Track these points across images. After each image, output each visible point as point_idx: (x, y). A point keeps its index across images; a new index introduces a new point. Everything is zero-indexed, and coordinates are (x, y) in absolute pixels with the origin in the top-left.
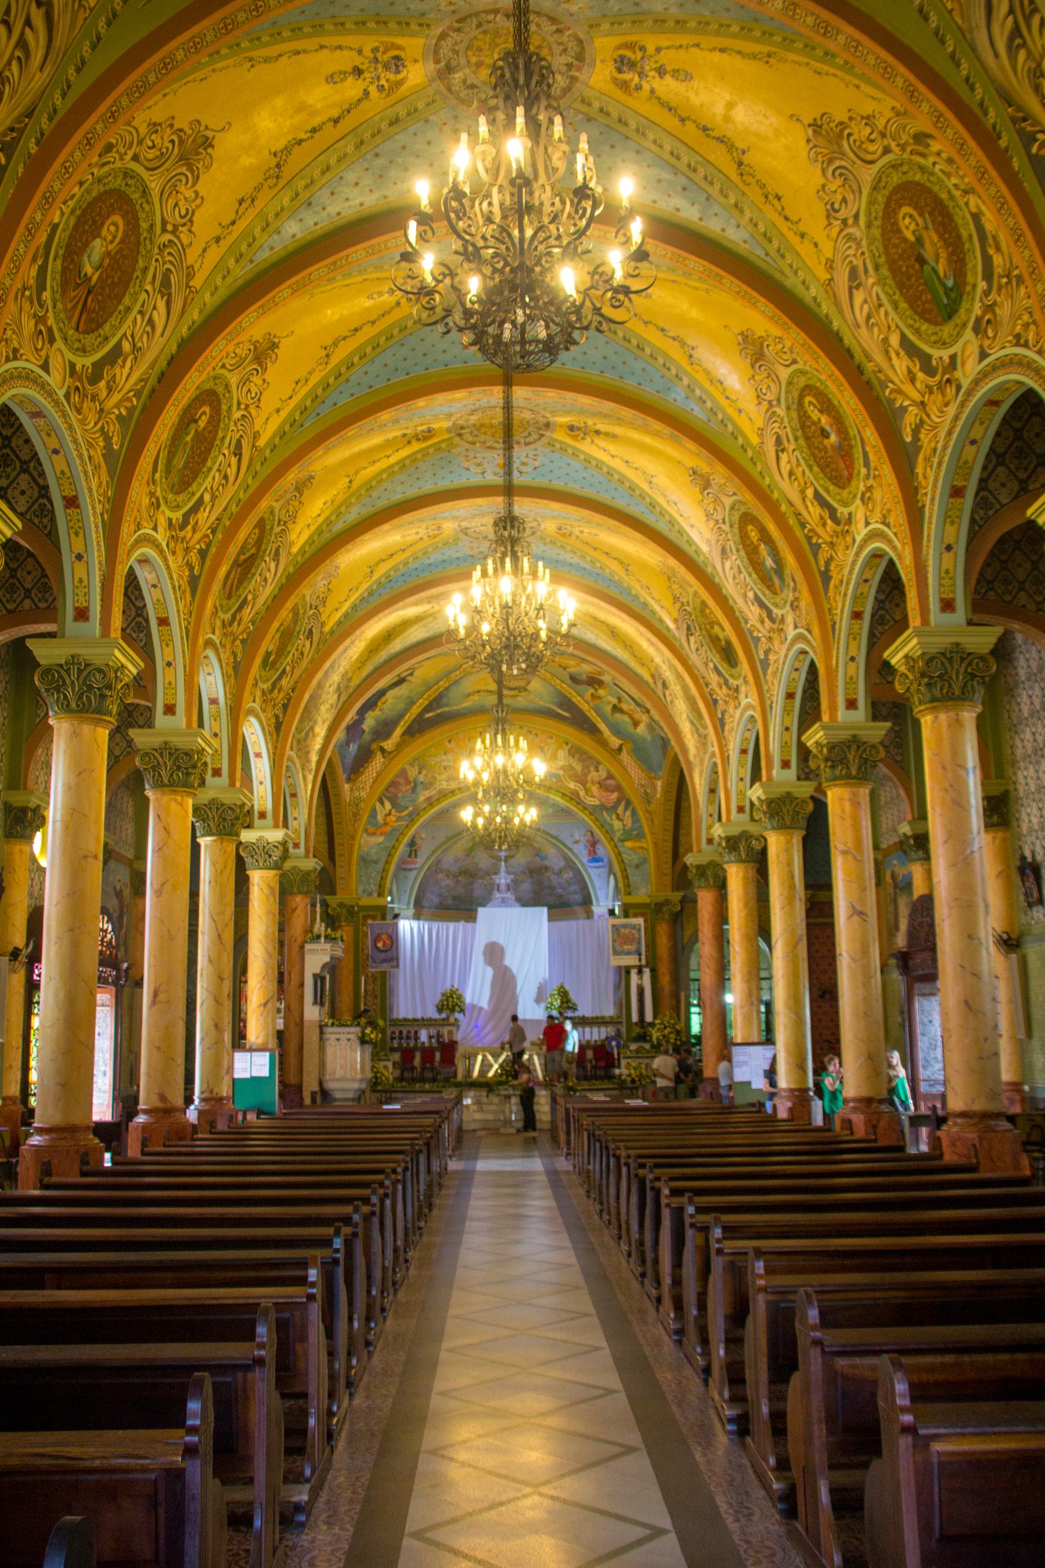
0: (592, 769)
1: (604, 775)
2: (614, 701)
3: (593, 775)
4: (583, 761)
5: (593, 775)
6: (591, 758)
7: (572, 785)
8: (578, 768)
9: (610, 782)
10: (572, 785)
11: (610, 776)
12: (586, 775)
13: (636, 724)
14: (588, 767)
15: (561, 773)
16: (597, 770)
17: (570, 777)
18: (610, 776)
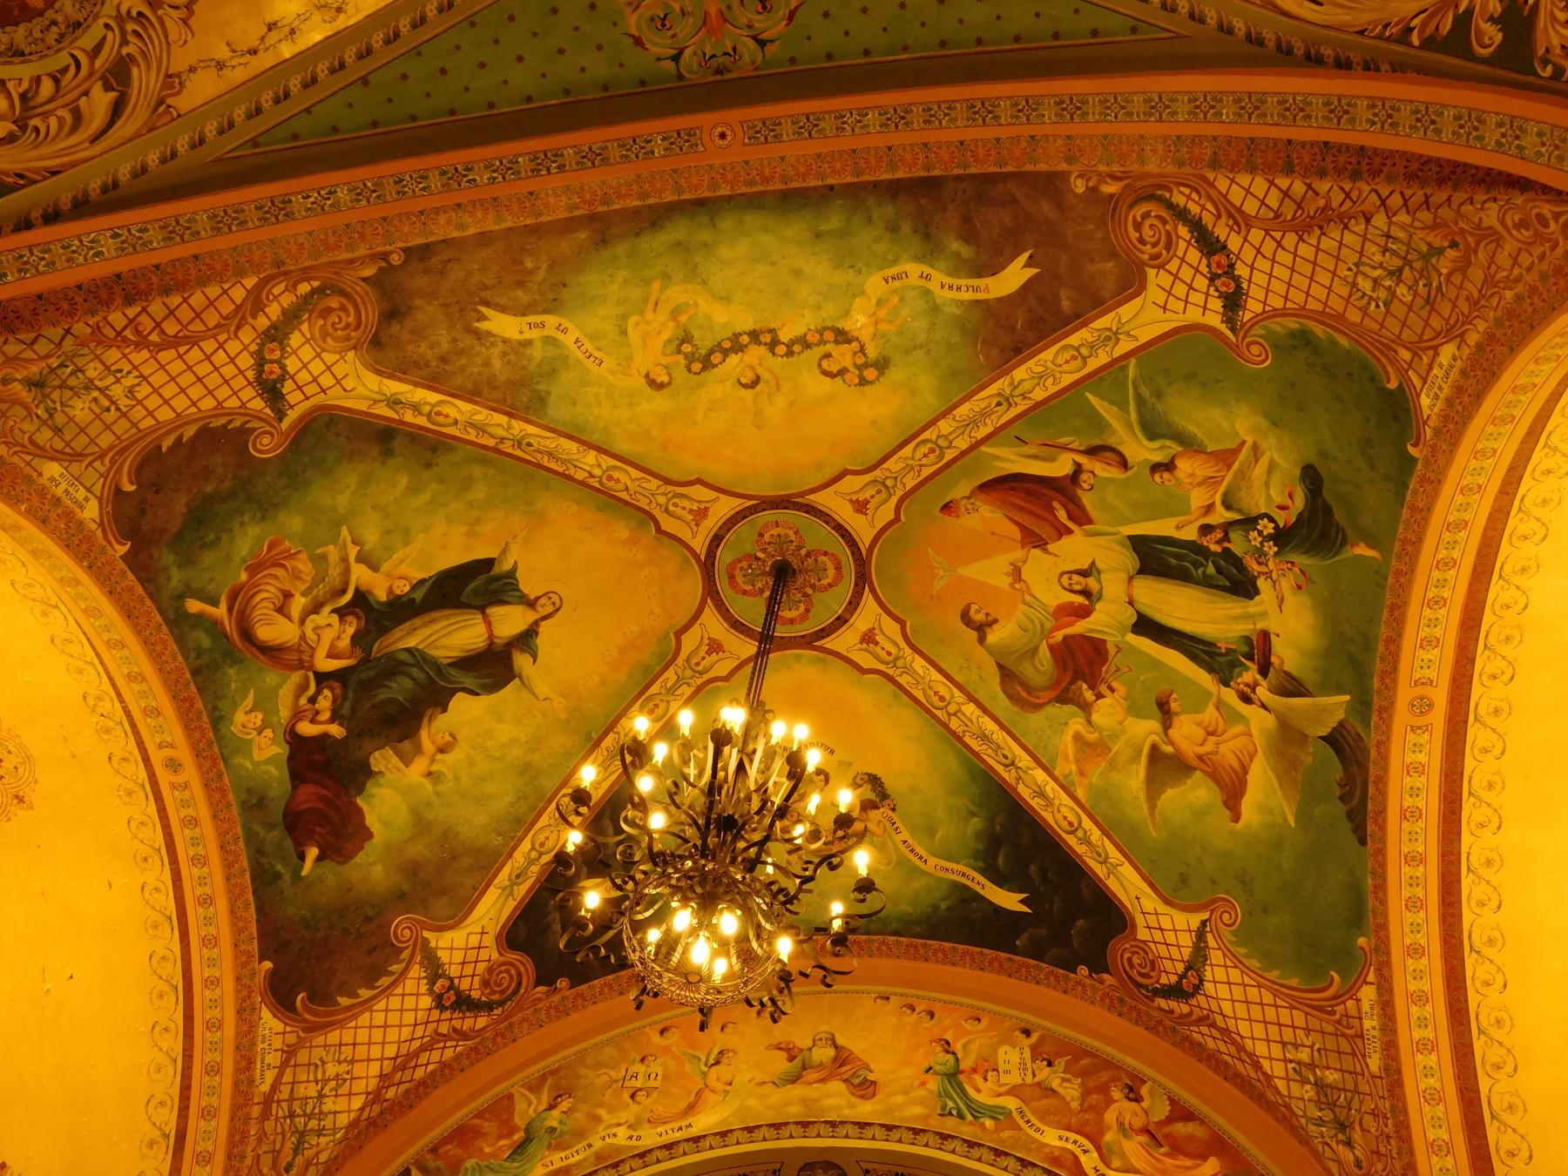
0: (1116, 1094)
1: (1162, 1110)
2: (1146, 729)
3: (1120, 1109)
4: (1084, 1074)
5: (1120, 1109)
6: (1110, 1065)
7: (1052, 1137)
8: (1071, 1092)
9: (1181, 1129)
10: (1052, 1137)
11: (1181, 1113)
12: (1099, 1111)
13: (1233, 792)
14: (1104, 1089)
15: (1011, 1103)
16: (1133, 1095)
17: (1043, 1116)
18: (1181, 1113)
